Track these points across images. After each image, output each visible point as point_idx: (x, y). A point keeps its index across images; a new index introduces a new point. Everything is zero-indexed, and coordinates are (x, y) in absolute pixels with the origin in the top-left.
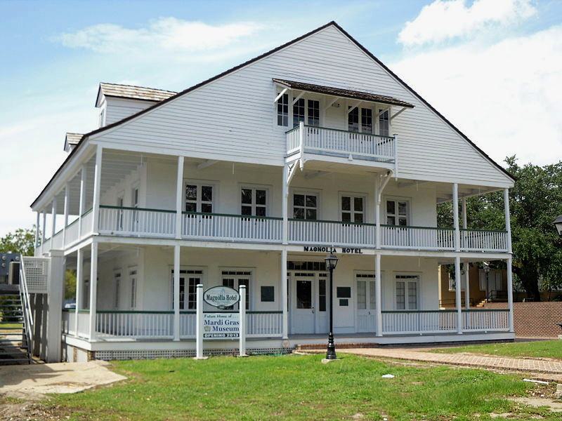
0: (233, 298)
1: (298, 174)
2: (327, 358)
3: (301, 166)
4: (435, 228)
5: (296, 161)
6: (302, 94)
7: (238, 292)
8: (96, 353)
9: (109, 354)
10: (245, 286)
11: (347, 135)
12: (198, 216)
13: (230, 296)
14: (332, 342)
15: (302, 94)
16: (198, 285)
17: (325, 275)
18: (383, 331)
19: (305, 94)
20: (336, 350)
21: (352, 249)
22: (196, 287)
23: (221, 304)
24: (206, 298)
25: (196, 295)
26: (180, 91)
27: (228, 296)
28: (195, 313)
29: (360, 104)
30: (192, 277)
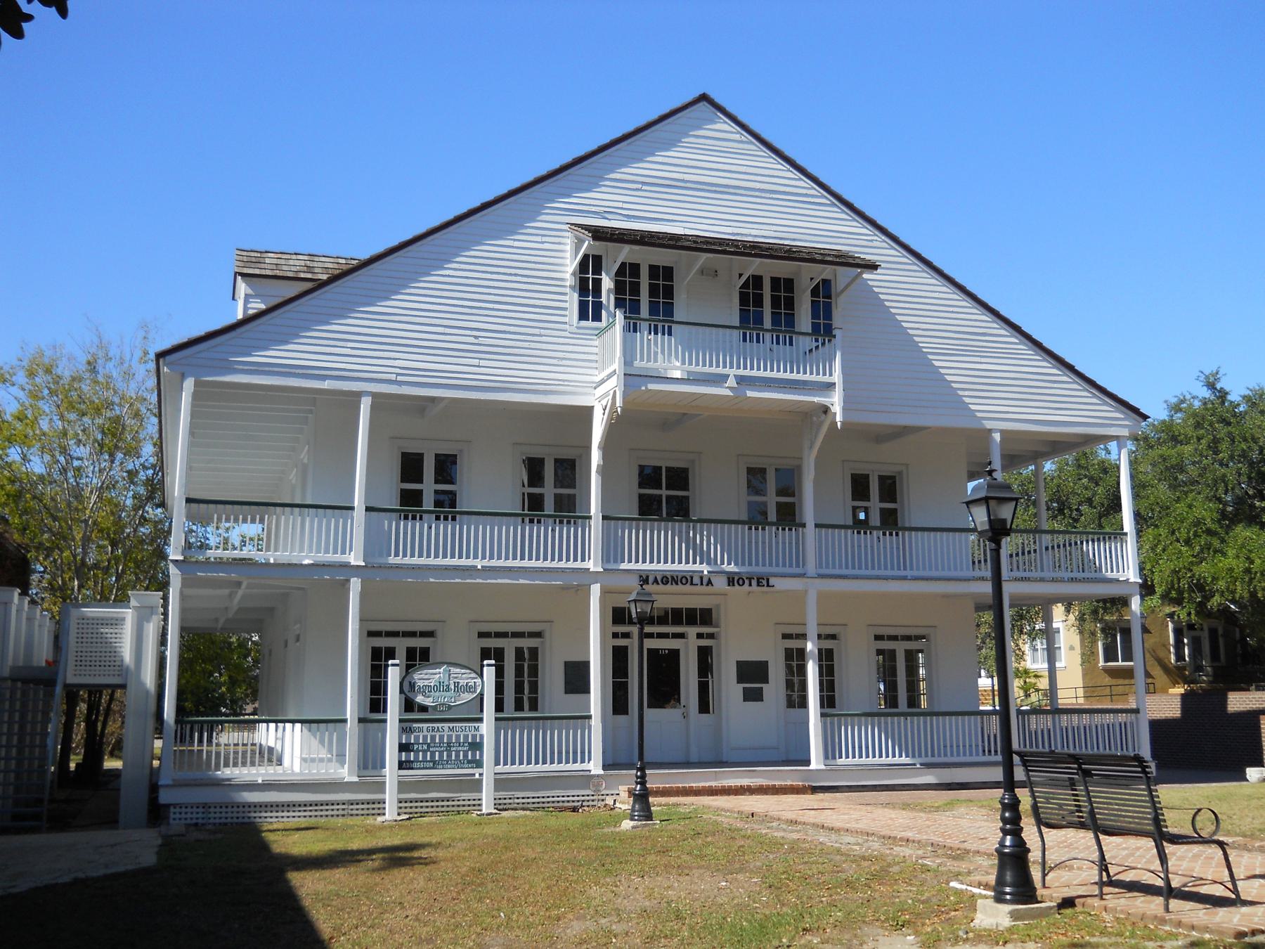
0: (469, 689)
1: (616, 426)
2: (632, 819)
3: (619, 403)
4: (743, 523)
5: (612, 392)
6: (625, 253)
7: (481, 676)
8: (172, 809)
9: (201, 810)
10: (493, 662)
11: (737, 334)
12: (425, 516)
13: (463, 682)
14: (643, 783)
15: (625, 253)
16: (390, 662)
17: (626, 635)
18: (497, 763)
19: (629, 251)
20: (651, 799)
21: (750, 579)
22: (387, 666)
23: (441, 700)
24: (406, 688)
25: (386, 683)
26: (365, 255)
27: (456, 684)
28: (385, 721)
29: (646, 257)
30: (377, 645)
